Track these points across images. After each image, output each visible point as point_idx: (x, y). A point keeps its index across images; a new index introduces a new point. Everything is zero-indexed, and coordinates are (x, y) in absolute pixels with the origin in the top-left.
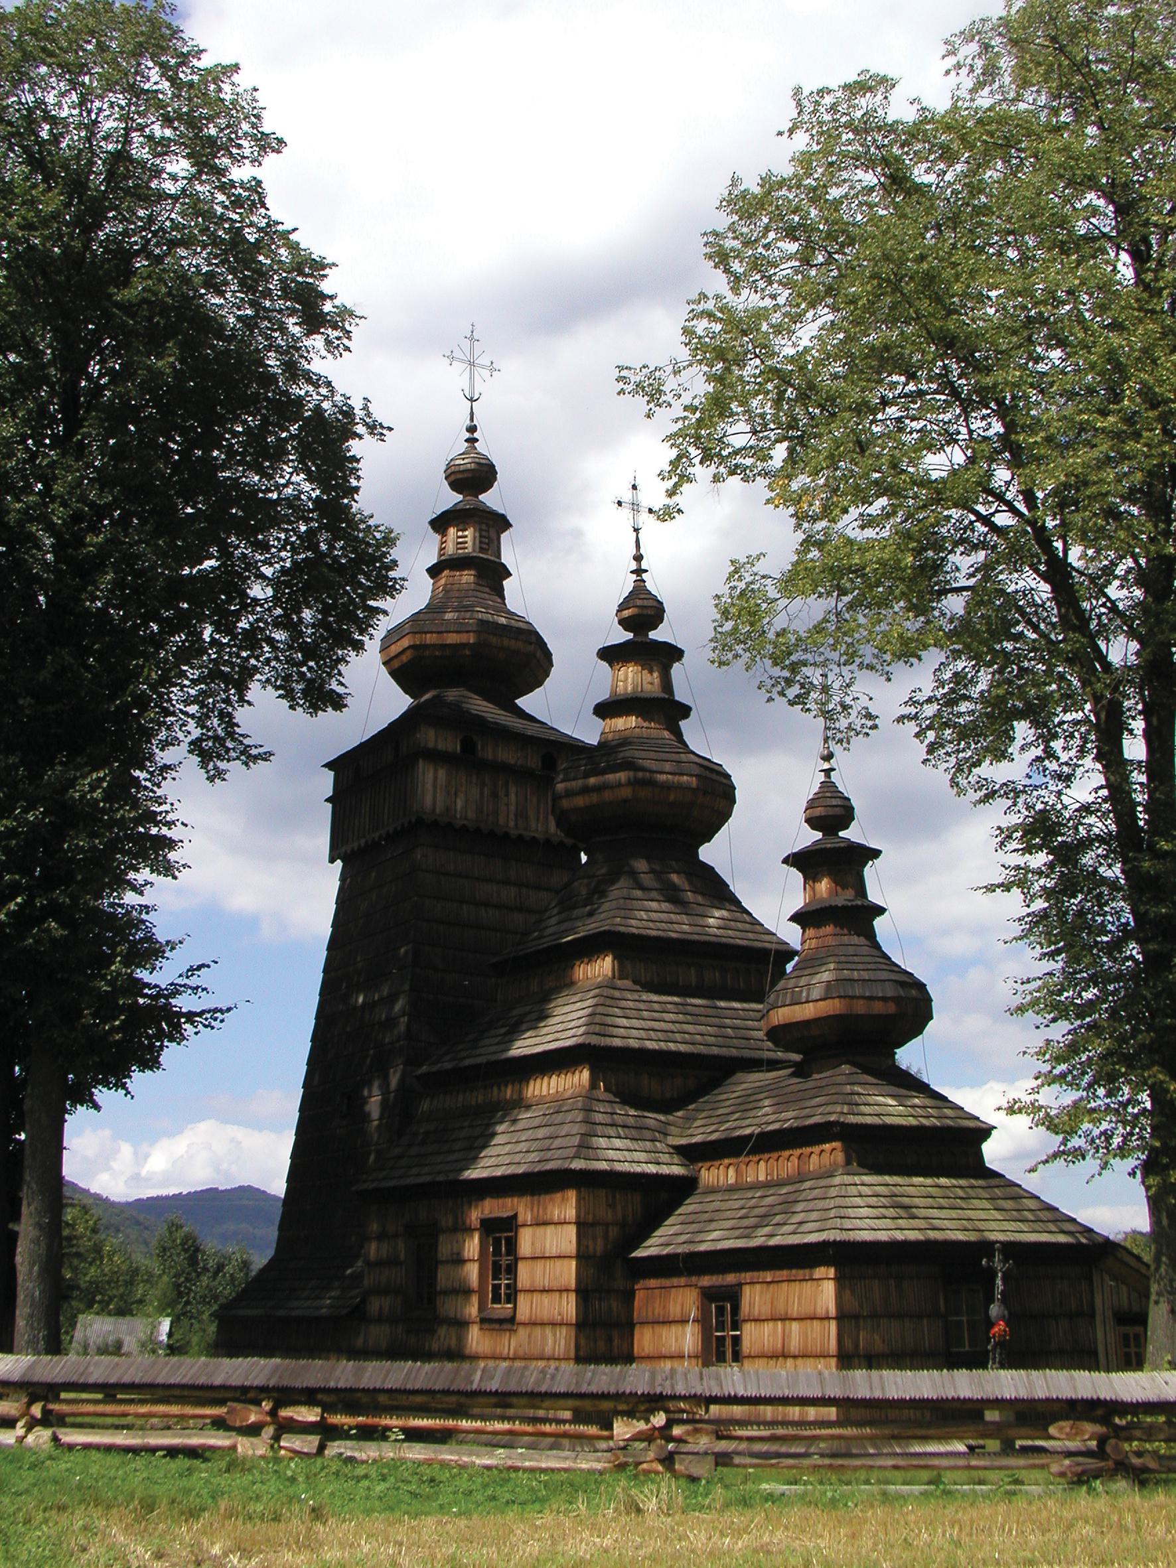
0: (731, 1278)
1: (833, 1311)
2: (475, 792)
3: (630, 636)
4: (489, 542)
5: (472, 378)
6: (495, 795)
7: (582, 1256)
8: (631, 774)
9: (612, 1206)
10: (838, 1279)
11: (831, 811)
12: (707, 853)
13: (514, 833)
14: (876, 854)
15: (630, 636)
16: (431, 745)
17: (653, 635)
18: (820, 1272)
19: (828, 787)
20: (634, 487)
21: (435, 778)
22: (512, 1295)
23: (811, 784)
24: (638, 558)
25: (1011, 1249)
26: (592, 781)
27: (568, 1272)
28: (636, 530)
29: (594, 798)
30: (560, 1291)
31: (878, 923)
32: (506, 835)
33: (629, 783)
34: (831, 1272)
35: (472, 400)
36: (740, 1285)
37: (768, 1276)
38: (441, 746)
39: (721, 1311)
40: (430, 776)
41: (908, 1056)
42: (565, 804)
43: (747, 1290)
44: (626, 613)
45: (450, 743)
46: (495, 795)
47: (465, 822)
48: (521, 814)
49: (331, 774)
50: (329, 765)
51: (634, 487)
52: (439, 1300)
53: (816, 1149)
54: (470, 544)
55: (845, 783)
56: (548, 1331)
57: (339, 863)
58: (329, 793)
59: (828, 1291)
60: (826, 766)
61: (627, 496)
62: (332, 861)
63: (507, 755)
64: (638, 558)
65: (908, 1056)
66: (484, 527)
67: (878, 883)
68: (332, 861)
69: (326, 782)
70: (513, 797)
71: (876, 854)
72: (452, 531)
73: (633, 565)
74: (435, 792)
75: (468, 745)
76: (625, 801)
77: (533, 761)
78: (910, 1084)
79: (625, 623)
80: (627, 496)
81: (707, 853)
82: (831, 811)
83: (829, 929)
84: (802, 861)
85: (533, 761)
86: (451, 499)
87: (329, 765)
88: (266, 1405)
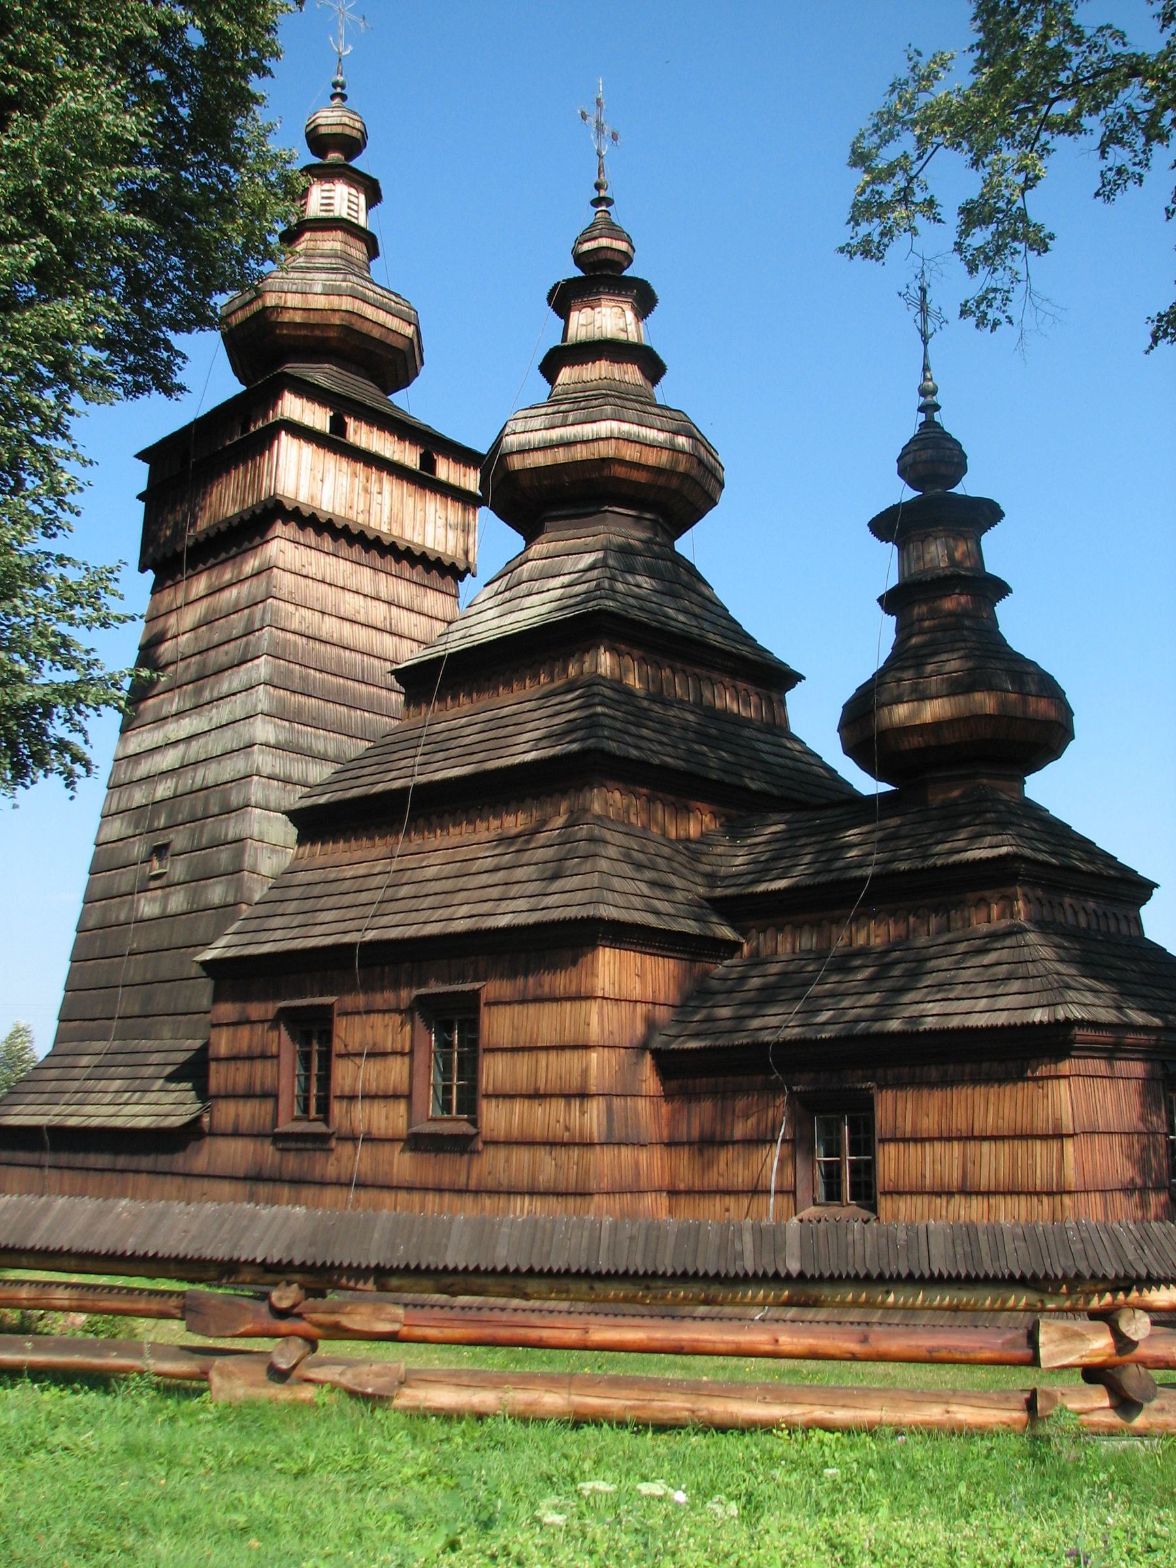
11: (932, 458)
20: (598, 102)
23: (909, 425)
29: (561, 456)
30: (567, 1096)
42: (517, 463)
44: (587, 246)
45: (318, 418)
49: (145, 467)
50: (143, 456)
52: (337, 1109)
56: (542, 1154)
57: (150, 575)
58: (143, 487)
62: (142, 569)
65: (1044, 787)
68: (142, 569)
69: (140, 476)
70: (386, 494)
75: (338, 425)
77: (410, 456)
81: (684, 545)
82: (932, 458)
87: (143, 456)
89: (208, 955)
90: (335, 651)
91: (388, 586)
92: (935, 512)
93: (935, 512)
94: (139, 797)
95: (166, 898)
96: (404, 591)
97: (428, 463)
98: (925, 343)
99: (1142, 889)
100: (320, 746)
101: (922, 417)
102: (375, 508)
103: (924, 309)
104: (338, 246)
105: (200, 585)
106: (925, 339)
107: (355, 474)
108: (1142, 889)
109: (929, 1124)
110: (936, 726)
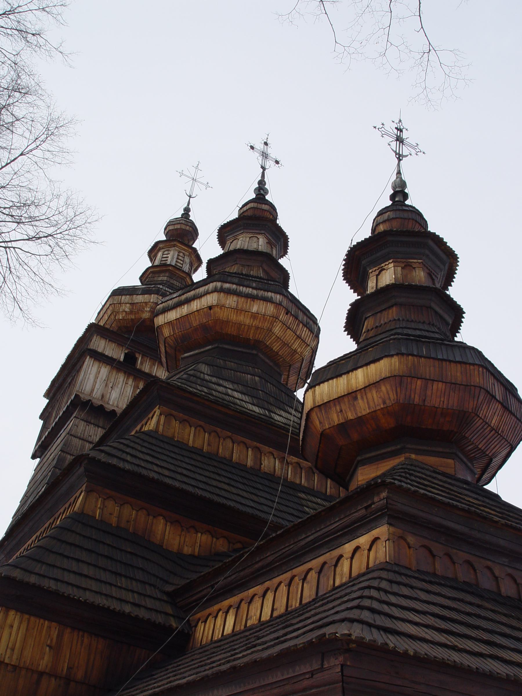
5: (192, 186)
8: (219, 284)
16: (100, 350)
20: (266, 144)
21: (98, 372)
28: (264, 168)
35: (190, 197)
40: (95, 369)
45: (118, 353)
47: (115, 409)
51: (266, 144)
53: (348, 548)
61: (259, 146)
62: (34, 457)
66: (181, 254)
68: (34, 457)
72: (160, 254)
74: (95, 382)
75: (130, 359)
76: (210, 308)
98: (400, 160)
104: (165, 278)
106: (400, 157)
110: (352, 395)
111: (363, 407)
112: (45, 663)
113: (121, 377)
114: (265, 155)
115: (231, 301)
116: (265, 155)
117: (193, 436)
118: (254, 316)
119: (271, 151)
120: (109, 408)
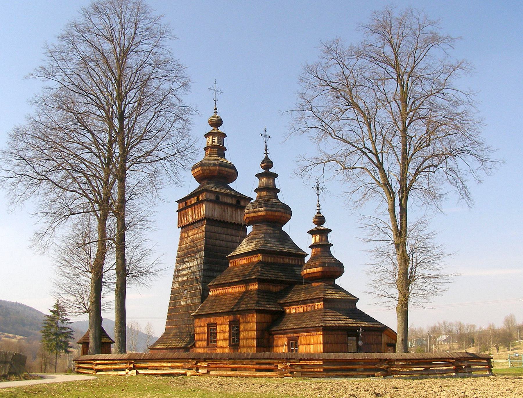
0: (295, 335)
1: (322, 342)
2: (219, 210)
3: (264, 171)
4: (221, 141)
6: (224, 211)
7: (257, 330)
9: (264, 318)
10: (323, 335)
11: (320, 220)
12: (285, 228)
13: (229, 221)
14: (331, 231)
15: (264, 171)
17: (270, 170)
18: (319, 333)
19: (319, 213)
20: (265, 131)
22: (238, 340)
24: (266, 150)
25: (364, 328)
26: (255, 210)
27: (254, 334)
31: (331, 248)
32: (227, 222)
33: (265, 210)
34: (322, 333)
36: (298, 337)
37: (305, 334)
38: (211, 198)
39: (292, 343)
41: (337, 282)
43: (300, 338)
44: (264, 164)
46: (224, 211)
48: (231, 216)
51: (265, 131)
52: (217, 342)
53: (317, 304)
54: (216, 142)
55: (323, 213)
59: (321, 337)
60: (318, 208)
61: (263, 133)
63: (228, 200)
64: (266, 150)
65: (337, 282)
67: (331, 238)
69: (177, 206)
71: (331, 231)
72: (211, 137)
73: (265, 152)
75: (217, 198)
77: (234, 202)
78: (338, 289)
79: (263, 168)
80: (263, 133)
81: (285, 228)
82: (320, 220)
83: (319, 249)
84: (312, 232)
85: (234, 202)
86: (210, 129)
88: (194, 363)
89: (193, 314)
90: (218, 248)
91: (230, 231)
92: (320, 230)
93: (320, 230)
94: (180, 279)
95: (187, 301)
96: (233, 232)
97: (238, 202)
99: (357, 300)
100: (216, 268)
101: (317, 211)
102: (227, 214)
103: (318, 189)
105: (191, 233)
106: (318, 195)
107: (221, 208)
108: (357, 300)
109: (305, 342)
111: (315, 275)
112: (264, 321)
113: (216, 206)
114: (265, 136)
115: (269, 213)
116: (265, 136)
117: (269, 259)
118: (276, 216)
119: (268, 134)
120: (215, 219)
